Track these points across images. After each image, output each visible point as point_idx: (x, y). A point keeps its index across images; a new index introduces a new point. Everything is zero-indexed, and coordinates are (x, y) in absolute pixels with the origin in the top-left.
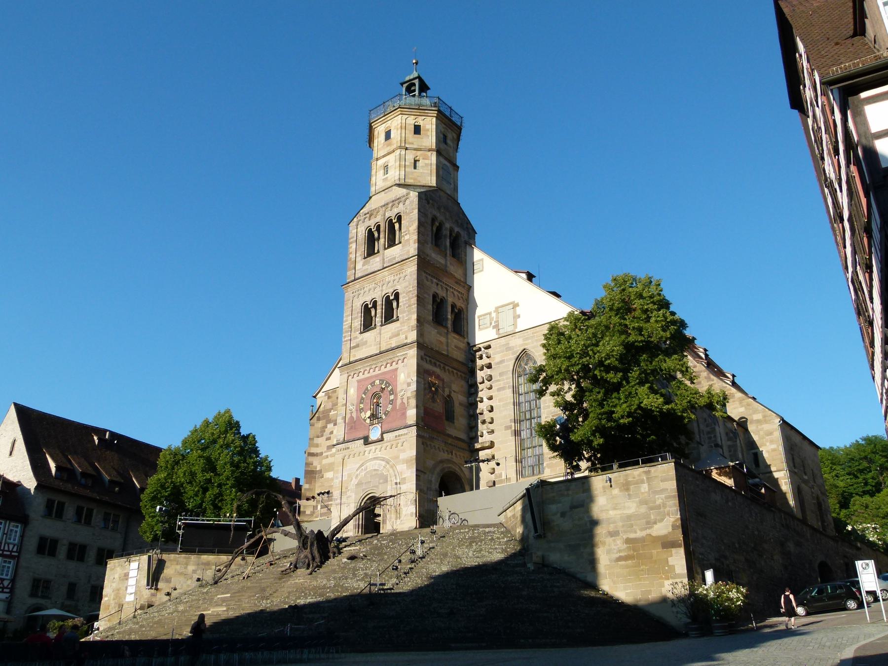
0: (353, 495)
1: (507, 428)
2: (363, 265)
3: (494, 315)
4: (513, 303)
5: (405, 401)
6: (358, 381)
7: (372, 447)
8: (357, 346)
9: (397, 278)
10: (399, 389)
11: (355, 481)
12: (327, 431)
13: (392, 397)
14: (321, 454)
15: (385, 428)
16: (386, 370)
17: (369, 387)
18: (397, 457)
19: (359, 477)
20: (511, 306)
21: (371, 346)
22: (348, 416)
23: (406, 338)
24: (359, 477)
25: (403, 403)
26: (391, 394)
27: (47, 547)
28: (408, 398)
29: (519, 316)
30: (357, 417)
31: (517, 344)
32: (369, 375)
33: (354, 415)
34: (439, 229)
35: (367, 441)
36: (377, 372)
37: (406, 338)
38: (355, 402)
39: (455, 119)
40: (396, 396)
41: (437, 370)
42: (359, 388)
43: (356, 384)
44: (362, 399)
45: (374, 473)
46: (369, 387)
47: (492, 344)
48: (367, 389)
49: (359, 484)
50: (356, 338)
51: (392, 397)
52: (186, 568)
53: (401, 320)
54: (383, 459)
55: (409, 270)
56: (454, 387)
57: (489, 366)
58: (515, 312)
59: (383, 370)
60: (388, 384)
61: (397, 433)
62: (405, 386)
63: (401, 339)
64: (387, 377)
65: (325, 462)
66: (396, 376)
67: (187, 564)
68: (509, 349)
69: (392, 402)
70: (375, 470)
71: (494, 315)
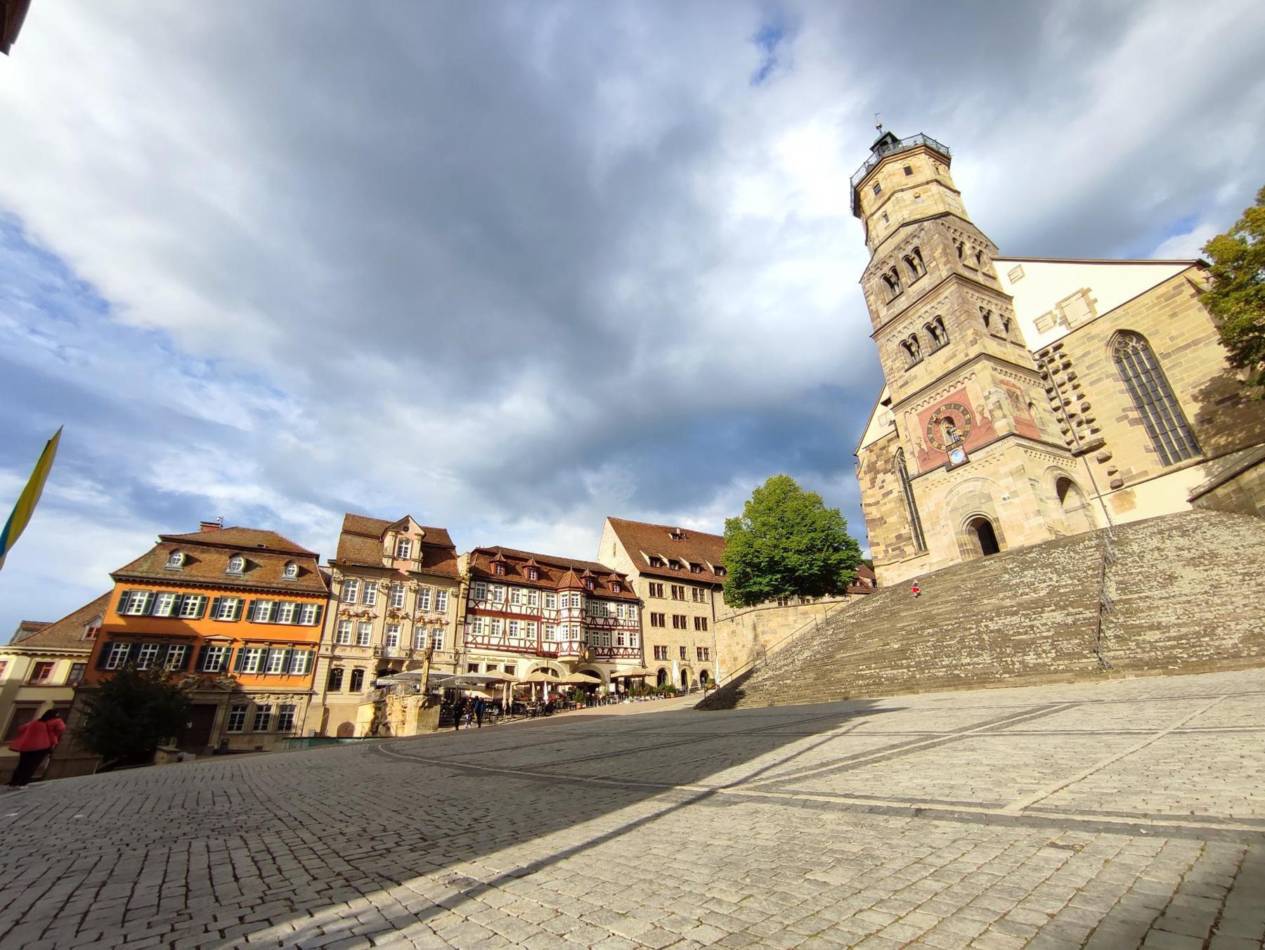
0: (949, 522)
1: (1119, 419)
3: (1057, 312)
5: (987, 414)
7: (954, 473)
8: (906, 383)
10: (974, 405)
11: (946, 509)
12: (878, 481)
14: (878, 503)
15: (969, 448)
22: (917, 449)
23: (967, 355)
25: (984, 418)
27: (657, 620)
28: (991, 412)
29: (1096, 301)
31: (1106, 329)
33: (924, 446)
34: (960, 250)
37: (967, 355)
39: (942, 150)
40: (973, 413)
41: (1011, 380)
47: (1064, 341)
49: (954, 510)
54: (977, 479)
55: (947, 293)
56: (1033, 394)
57: (1067, 366)
60: (957, 406)
62: (982, 401)
63: (961, 358)
64: (955, 400)
65: (883, 509)
68: (1091, 338)
71: (1057, 312)
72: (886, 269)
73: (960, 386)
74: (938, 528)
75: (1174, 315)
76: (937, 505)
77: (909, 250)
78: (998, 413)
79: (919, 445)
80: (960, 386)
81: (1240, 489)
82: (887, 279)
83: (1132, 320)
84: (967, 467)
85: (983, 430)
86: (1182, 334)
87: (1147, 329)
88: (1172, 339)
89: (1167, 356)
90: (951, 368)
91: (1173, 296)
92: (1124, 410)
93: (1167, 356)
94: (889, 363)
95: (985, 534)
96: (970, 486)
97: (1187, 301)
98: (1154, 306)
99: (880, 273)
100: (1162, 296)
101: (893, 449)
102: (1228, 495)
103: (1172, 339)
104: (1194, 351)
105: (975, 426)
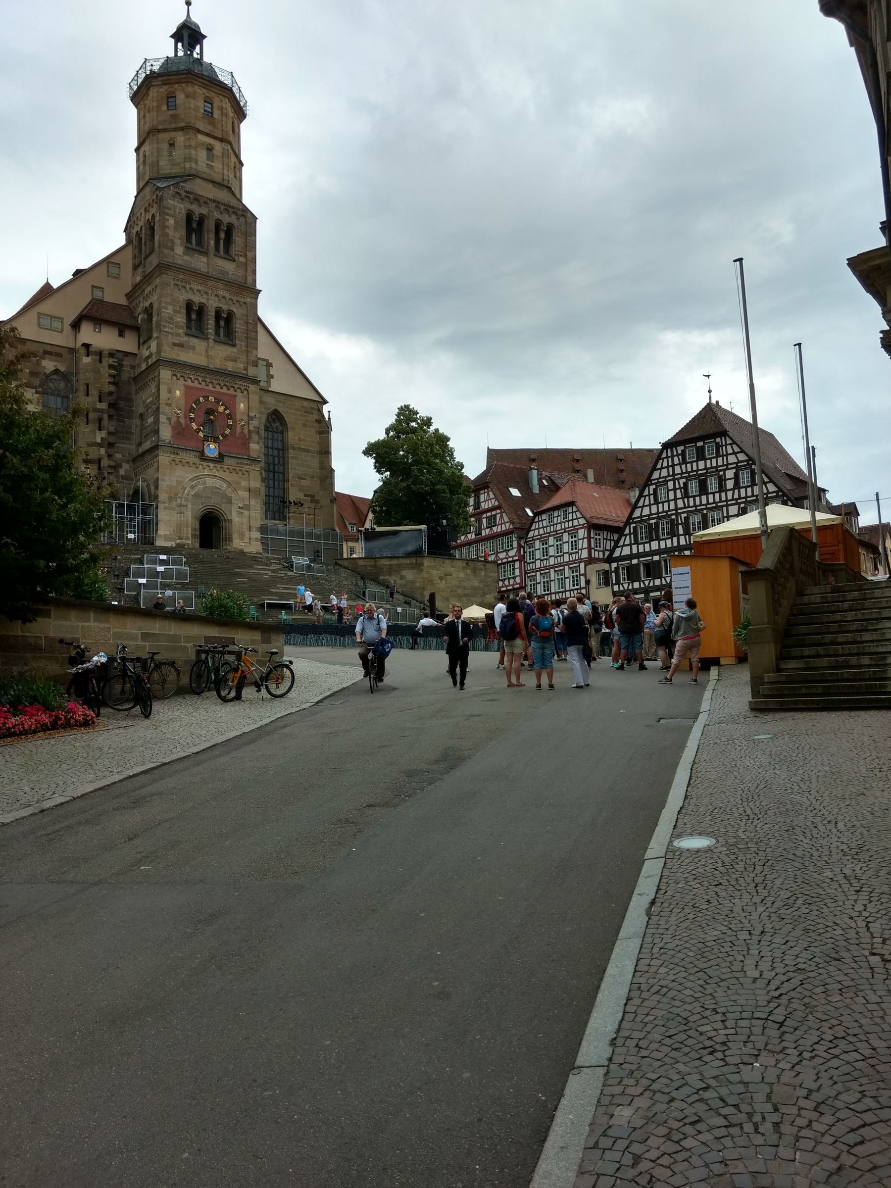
0: (190, 505)
4: (267, 361)
5: (246, 431)
6: (186, 387)
8: (181, 345)
9: (235, 298)
10: (238, 417)
13: (230, 422)
16: (222, 391)
17: (201, 399)
20: (265, 363)
22: (174, 419)
29: (272, 377)
30: (186, 424)
32: (200, 386)
33: (182, 421)
35: (203, 457)
36: (210, 387)
38: (183, 408)
40: (235, 422)
46: (201, 399)
49: (196, 496)
50: (178, 335)
51: (230, 422)
53: (238, 347)
58: (268, 371)
62: (246, 418)
69: (230, 427)
72: (197, 210)
73: (231, 391)
74: (174, 504)
75: (305, 425)
77: (226, 219)
78: (255, 437)
80: (231, 391)
81: (375, 566)
84: (219, 466)
89: (294, 448)
91: (308, 413)
93: (294, 448)
94: (170, 310)
95: (211, 527)
96: (218, 483)
98: (299, 410)
101: (49, 365)
102: (365, 566)
105: (233, 433)
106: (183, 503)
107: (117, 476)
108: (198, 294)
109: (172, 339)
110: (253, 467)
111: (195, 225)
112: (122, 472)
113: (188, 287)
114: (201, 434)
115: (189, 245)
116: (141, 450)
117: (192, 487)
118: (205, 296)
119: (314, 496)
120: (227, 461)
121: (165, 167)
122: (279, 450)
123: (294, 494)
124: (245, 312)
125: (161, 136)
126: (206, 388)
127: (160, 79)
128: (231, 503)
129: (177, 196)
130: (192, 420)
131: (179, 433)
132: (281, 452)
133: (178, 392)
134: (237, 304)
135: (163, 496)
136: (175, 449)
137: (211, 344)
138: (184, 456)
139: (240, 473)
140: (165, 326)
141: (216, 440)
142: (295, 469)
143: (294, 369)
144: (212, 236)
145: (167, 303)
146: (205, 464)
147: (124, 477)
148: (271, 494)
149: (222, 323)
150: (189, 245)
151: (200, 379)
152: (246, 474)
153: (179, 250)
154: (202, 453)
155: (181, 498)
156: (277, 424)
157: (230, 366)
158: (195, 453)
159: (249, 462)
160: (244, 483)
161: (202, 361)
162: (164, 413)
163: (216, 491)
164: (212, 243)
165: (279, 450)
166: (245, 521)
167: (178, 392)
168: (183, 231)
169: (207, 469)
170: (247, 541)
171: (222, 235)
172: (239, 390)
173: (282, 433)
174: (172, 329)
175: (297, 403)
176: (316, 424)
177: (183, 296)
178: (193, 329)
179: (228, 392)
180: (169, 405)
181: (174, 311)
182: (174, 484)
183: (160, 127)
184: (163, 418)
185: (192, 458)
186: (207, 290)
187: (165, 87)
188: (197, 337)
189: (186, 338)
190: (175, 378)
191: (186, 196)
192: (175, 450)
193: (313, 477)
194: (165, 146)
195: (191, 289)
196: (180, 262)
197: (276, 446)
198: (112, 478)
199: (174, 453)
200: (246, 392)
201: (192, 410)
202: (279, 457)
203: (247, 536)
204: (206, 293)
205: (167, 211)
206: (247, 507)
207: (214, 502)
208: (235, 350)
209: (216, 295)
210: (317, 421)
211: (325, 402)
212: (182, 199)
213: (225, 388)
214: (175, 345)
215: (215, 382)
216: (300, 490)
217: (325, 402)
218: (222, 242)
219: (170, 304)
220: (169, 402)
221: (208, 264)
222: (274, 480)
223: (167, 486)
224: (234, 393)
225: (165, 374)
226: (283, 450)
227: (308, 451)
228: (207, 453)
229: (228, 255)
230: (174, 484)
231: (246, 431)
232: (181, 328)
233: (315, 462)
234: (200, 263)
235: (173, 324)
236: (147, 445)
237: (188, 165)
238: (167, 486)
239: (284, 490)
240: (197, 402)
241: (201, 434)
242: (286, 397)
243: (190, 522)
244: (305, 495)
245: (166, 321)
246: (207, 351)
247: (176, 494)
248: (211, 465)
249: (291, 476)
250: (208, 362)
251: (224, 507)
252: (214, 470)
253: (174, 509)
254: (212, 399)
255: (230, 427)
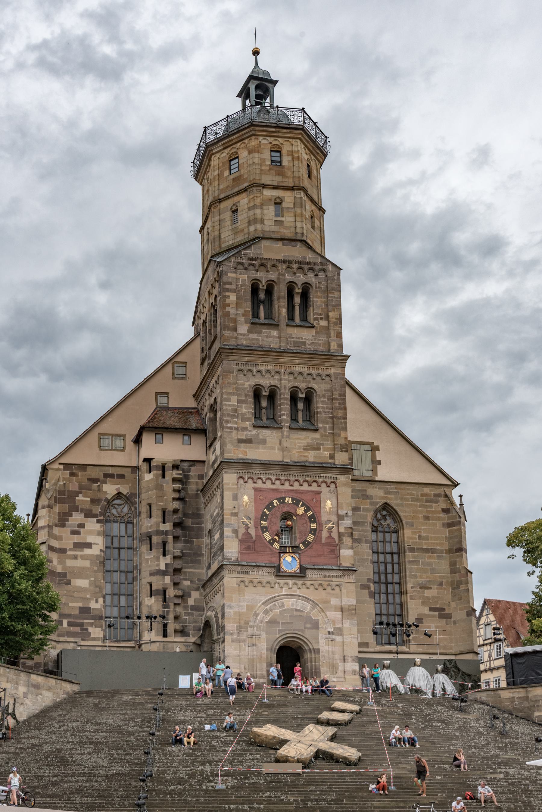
0: (264, 635)
2: (250, 331)
5: (335, 535)
6: (256, 490)
8: (249, 441)
10: (324, 518)
13: (314, 526)
16: (302, 488)
17: (275, 502)
18: (327, 602)
19: (272, 614)
21: (273, 448)
22: (242, 531)
24: (272, 614)
26: (311, 522)
28: (340, 535)
32: (273, 487)
35: (279, 573)
36: (287, 486)
38: (252, 516)
40: (320, 525)
42: (256, 500)
43: (252, 492)
44: (264, 514)
45: (295, 613)
46: (275, 502)
48: (272, 503)
49: (271, 622)
50: (245, 429)
51: (314, 526)
52: (16, 688)
54: (307, 599)
59: (296, 486)
61: (326, 573)
62: (334, 518)
66: (319, 501)
67: (17, 683)
69: (314, 532)
70: (297, 610)
74: (244, 635)
75: (427, 518)
76: (250, 608)
79: (247, 528)
82: (255, 289)
83: (399, 502)
84: (300, 583)
85: (326, 550)
86: (428, 540)
87: (406, 517)
88: (420, 537)
89: (412, 550)
90: (311, 460)
92: (369, 580)
94: (234, 400)
96: (299, 604)
97: (438, 512)
98: (417, 500)
99: (253, 274)
100: (426, 495)
103: (420, 537)
104: (429, 558)
105: (318, 540)
106: (256, 632)
107: (186, 608)
108: (268, 376)
109: (235, 435)
110: (346, 579)
111: (262, 296)
112: (191, 602)
113: (255, 370)
114: (276, 546)
115: (256, 320)
116: (210, 573)
117: (266, 612)
118: (277, 377)
119: (444, 609)
120: (310, 574)
121: (229, 238)
122: (392, 554)
123: (415, 610)
124: (328, 386)
125: (223, 205)
126: (281, 487)
127: (220, 144)
128: (317, 628)
129: (240, 267)
130: (264, 529)
131: (249, 548)
132: (395, 557)
133: (246, 498)
134: (318, 379)
135: (230, 626)
136: (242, 567)
137: (285, 433)
138: (254, 574)
139: (329, 589)
140: (227, 422)
141: (295, 549)
142: (415, 576)
143: (408, 448)
144: (284, 303)
145: (229, 394)
146: (282, 582)
147: (193, 608)
148: (384, 611)
149: (300, 405)
150: (256, 320)
151: (273, 478)
152: (337, 588)
153: (243, 329)
154: (278, 568)
155: (251, 627)
156: (389, 521)
157: (311, 457)
158: (269, 570)
159: (340, 573)
160: (334, 601)
161: (275, 456)
162: (229, 525)
163: (297, 614)
164: (284, 311)
165: (392, 554)
166: (337, 649)
167: (246, 498)
168: (248, 306)
169: (285, 587)
170: (342, 675)
171: (297, 299)
172: (324, 485)
173: (396, 532)
174: (236, 423)
175: (415, 491)
176: (442, 515)
177: (248, 383)
178: (264, 418)
179: (310, 489)
180: (235, 515)
181: (239, 401)
182: (244, 610)
183: (222, 196)
184: (228, 532)
185: (265, 575)
186: (278, 369)
187: (227, 151)
188: (267, 427)
189: (254, 432)
190: (241, 481)
191: (251, 264)
192: (244, 569)
193: (441, 584)
194: (227, 215)
195: (259, 371)
196: (244, 342)
197: (388, 549)
198: (179, 610)
199: (242, 572)
200: (333, 486)
201: (264, 517)
202: (393, 563)
203: (341, 668)
204: (278, 372)
205: (227, 287)
206: (339, 631)
207: (296, 628)
208: (317, 435)
209: (291, 373)
210: (444, 511)
211: (455, 485)
212: (246, 269)
213: (305, 484)
214: (240, 441)
215: (292, 479)
216: (423, 603)
217: (455, 485)
218: (297, 308)
219: (233, 394)
220: (236, 511)
221: (279, 337)
222: (387, 593)
223: (235, 613)
224: (318, 489)
225: (229, 478)
226: (398, 554)
227: (432, 551)
228: (285, 568)
229: (306, 323)
230: (244, 610)
231: (335, 535)
232: (249, 420)
233: (443, 565)
234: (270, 338)
235: (237, 417)
236: (215, 567)
237: (252, 229)
238: (235, 613)
239: (401, 605)
240: (270, 506)
241: (276, 546)
242: (399, 486)
243: (265, 656)
244: (431, 609)
245: (229, 415)
246: (280, 443)
247: (247, 623)
248: (290, 582)
249: (409, 586)
250: (283, 457)
251: (308, 634)
252: (295, 588)
253: (244, 641)
254: (289, 500)
255: (314, 532)
